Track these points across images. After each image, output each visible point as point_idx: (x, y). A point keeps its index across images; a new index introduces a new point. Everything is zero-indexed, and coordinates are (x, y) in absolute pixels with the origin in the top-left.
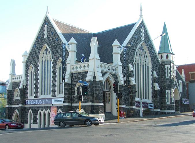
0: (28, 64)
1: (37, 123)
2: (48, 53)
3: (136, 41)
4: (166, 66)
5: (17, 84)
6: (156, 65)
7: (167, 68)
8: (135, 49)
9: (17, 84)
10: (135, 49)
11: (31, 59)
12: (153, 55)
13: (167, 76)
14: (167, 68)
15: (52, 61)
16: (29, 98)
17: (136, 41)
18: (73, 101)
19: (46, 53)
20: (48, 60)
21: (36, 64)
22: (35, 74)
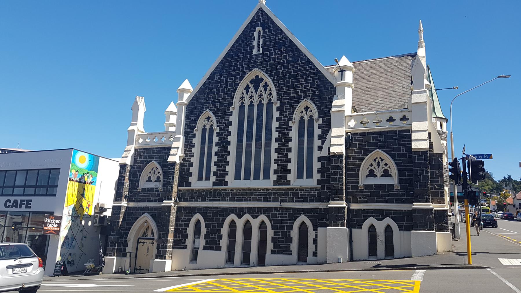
0: (193, 109)
1: (219, 249)
2: (261, 88)
5: (154, 153)
9: (154, 153)
11: (205, 99)
15: (278, 105)
16: (192, 185)
18: (351, 197)
19: (256, 88)
20: (260, 104)
21: (225, 110)
22: (217, 133)
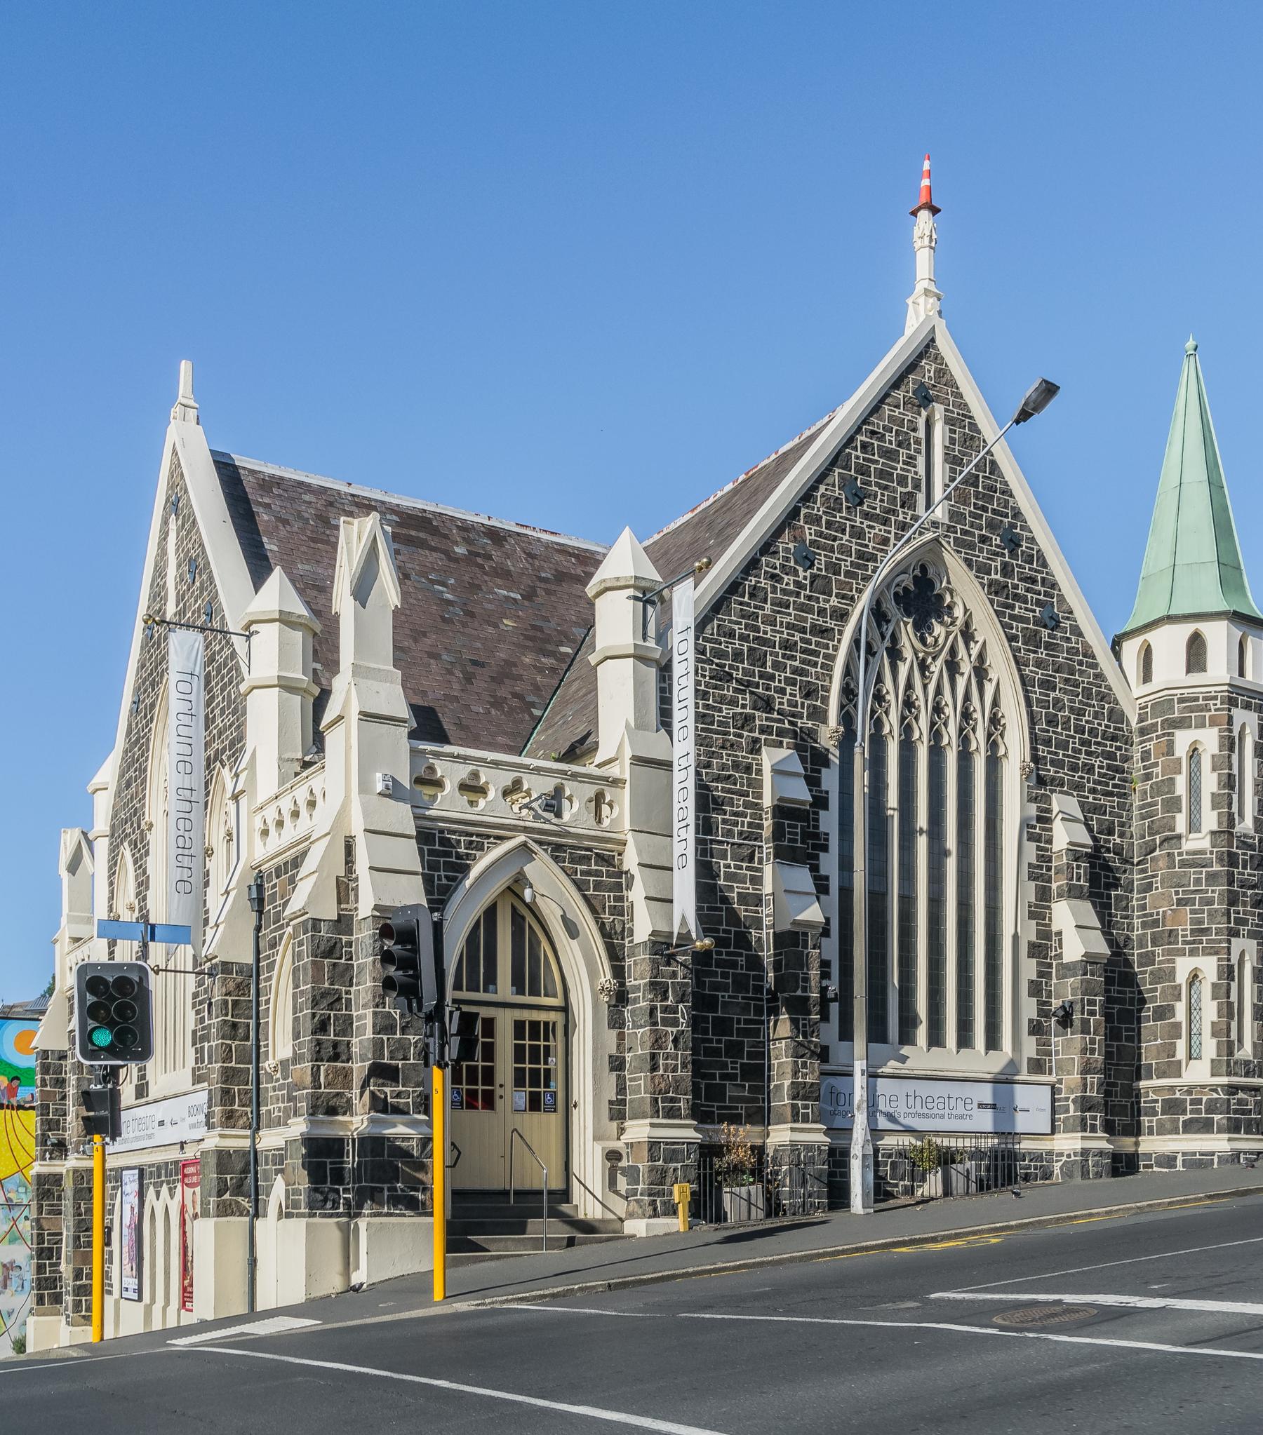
3: (858, 534)
4: (1183, 740)
6: (1084, 743)
7: (1194, 752)
8: (834, 601)
10: (834, 601)
12: (1048, 646)
13: (1194, 826)
14: (1194, 752)
17: (858, 534)
